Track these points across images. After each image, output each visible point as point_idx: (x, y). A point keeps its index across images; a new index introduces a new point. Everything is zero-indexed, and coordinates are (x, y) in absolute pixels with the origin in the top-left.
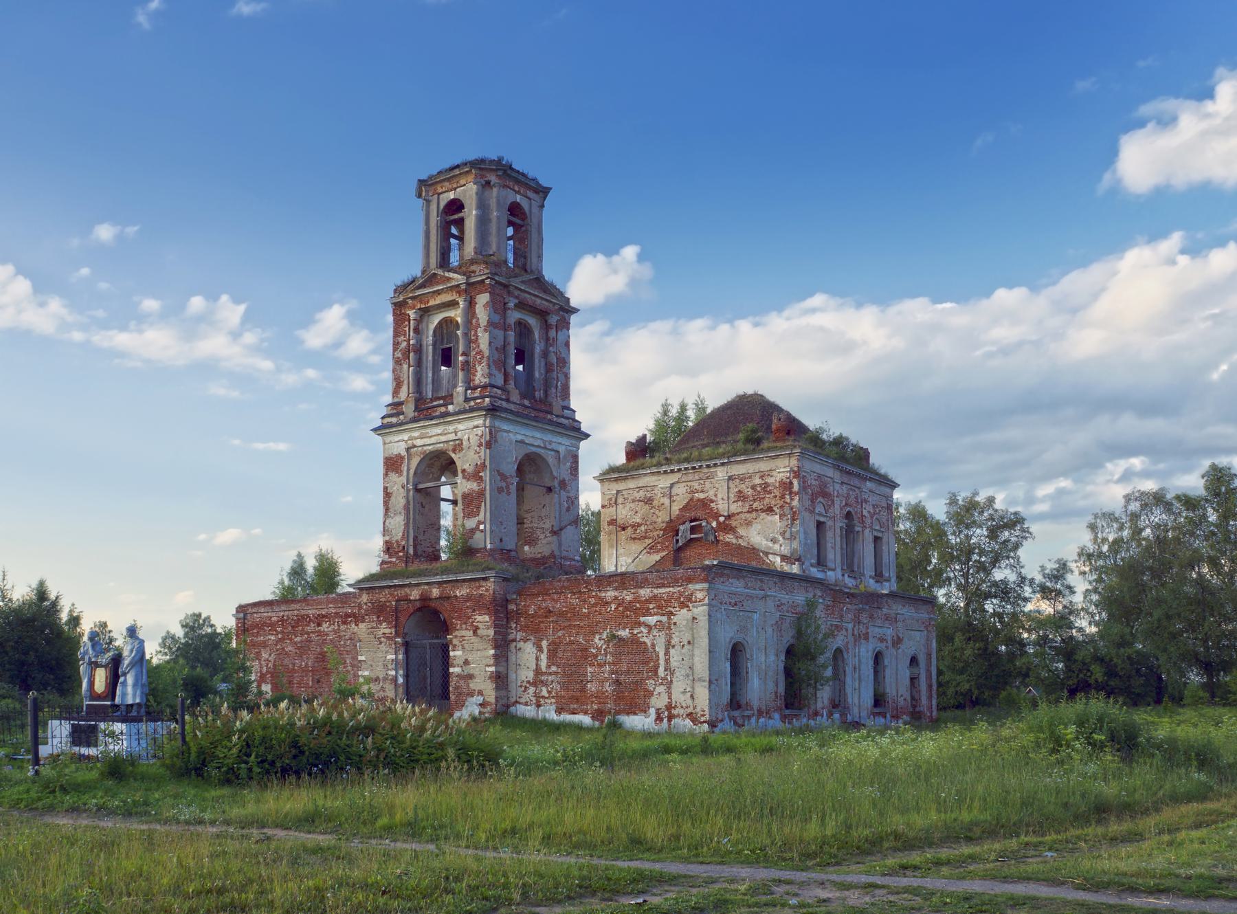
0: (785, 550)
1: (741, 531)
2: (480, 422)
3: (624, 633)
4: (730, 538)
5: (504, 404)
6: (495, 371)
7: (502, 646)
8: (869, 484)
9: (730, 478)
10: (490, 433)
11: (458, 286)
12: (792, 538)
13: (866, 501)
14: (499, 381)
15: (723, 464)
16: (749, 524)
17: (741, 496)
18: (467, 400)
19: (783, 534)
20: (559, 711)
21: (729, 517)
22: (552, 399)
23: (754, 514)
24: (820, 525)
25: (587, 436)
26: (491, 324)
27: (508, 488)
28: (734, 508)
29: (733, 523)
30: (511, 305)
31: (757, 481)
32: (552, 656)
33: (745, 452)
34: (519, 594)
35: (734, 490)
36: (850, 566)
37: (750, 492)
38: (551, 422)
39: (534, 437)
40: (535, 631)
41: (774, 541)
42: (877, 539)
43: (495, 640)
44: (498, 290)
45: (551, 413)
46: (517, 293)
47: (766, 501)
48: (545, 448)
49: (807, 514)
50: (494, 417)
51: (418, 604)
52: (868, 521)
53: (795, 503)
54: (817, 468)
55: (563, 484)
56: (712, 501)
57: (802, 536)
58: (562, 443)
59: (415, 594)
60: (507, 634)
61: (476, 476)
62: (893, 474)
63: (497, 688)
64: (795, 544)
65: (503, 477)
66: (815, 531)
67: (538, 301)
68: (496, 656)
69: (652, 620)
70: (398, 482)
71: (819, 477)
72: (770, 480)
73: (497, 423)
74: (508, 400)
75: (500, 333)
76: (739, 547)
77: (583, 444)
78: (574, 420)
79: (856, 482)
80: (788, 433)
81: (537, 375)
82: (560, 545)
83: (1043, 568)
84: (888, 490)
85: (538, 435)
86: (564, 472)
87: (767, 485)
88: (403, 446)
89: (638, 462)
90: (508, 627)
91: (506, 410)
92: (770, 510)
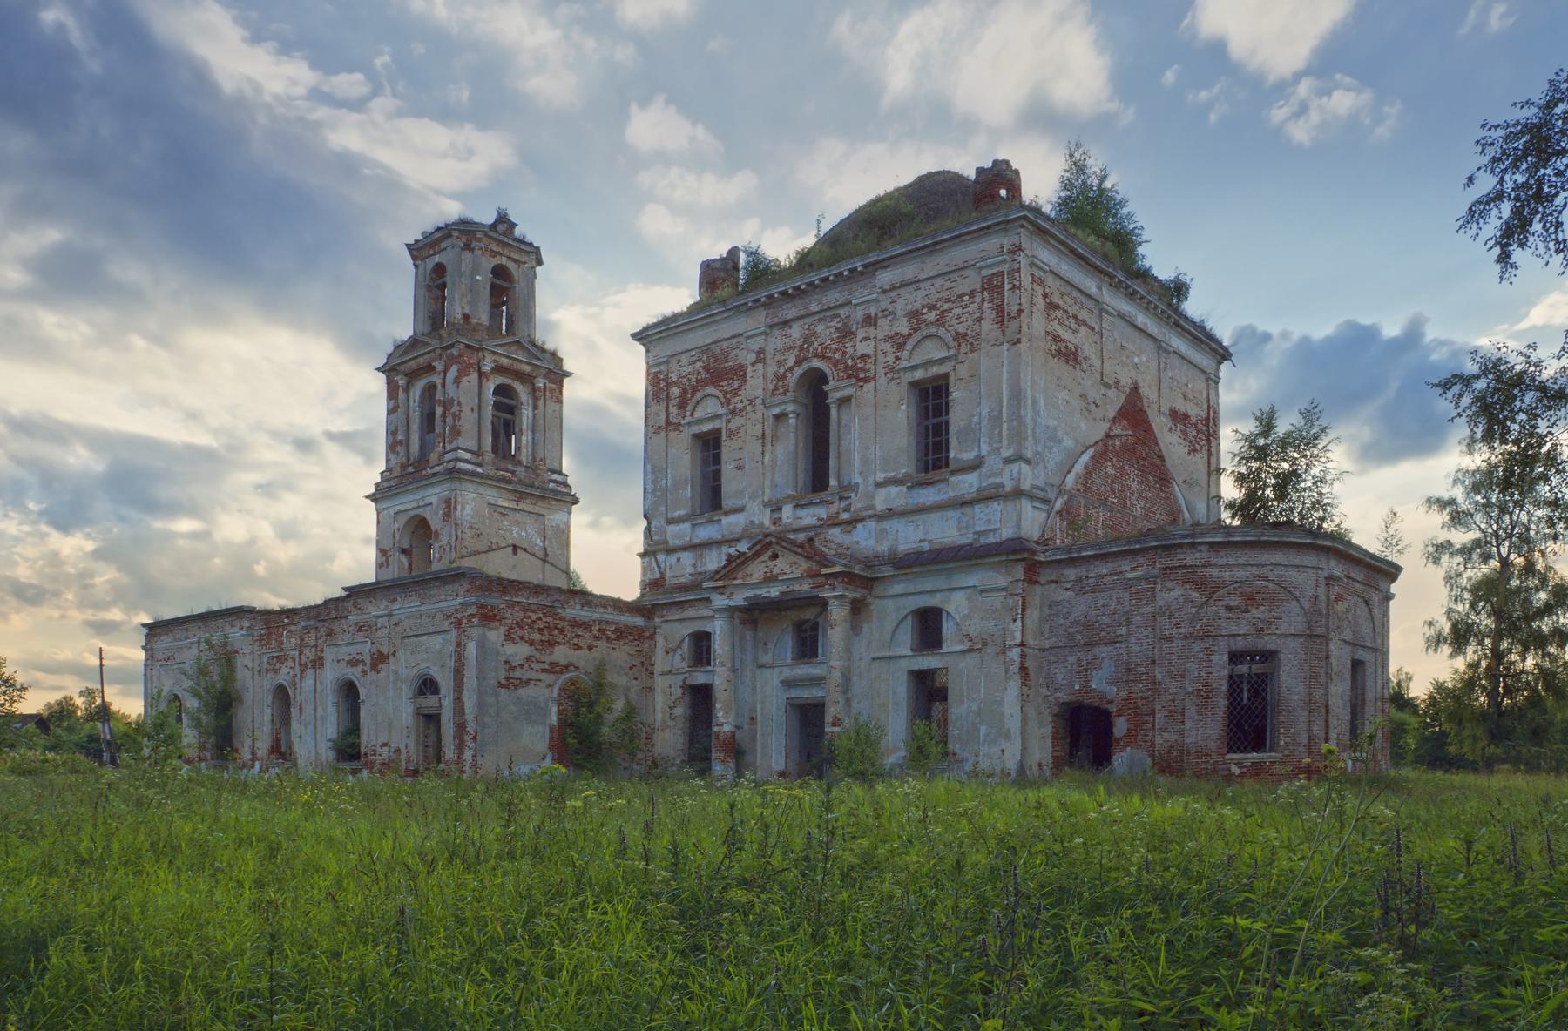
38: (428, 477)
85: (411, 497)
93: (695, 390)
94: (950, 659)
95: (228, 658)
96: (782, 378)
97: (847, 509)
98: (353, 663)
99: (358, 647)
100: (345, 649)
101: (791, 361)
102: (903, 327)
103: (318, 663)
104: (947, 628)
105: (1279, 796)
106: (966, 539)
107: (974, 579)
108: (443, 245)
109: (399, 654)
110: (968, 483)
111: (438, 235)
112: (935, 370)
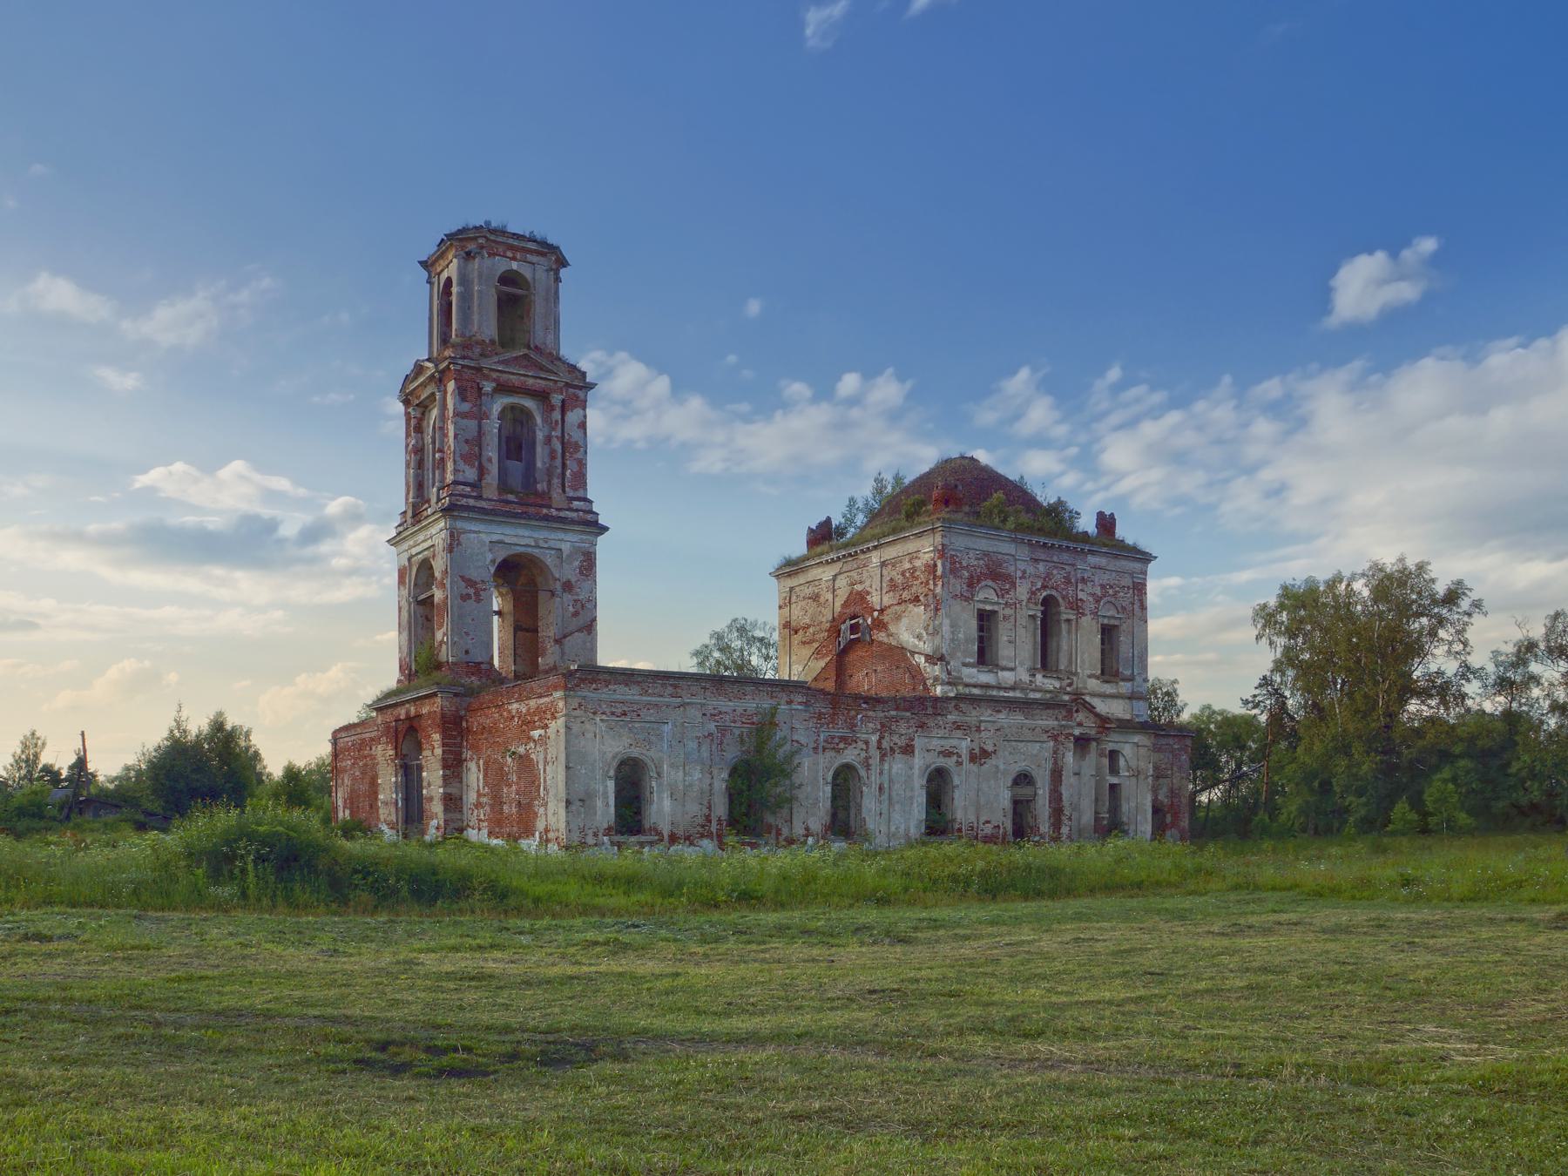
0: (927, 648)
1: (892, 628)
2: (442, 524)
3: (521, 750)
4: (881, 636)
5: (472, 502)
6: (462, 465)
7: (453, 766)
8: (1091, 559)
9: (883, 564)
10: (452, 535)
11: (432, 376)
12: (936, 632)
13: (1083, 580)
14: (470, 474)
15: (875, 547)
16: (898, 618)
17: (893, 586)
18: (439, 500)
19: (926, 629)
20: (490, 834)
21: (882, 611)
22: (556, 495)
23: (903, 607)
24: (986, 620)
25: (605, 529)
26: (456, 414)
27: (477, 594)
28: (887, 600)
29: (886, 618)
30: (488, 387)
31: (907, 566)
32: (485, 775)
33: (894, 531)
34: (467, 709)
35: (886, 579)
36: (1046, 660)
37: (899, 579)
38: (547, 518)
39: (519, 537)
40: (476, 748)
41: (919, 637)
42: (1108, 633)
43: (443, 759)
44: (468, 374)
45: (550, 507)
46: (495, 375)
47: (914, 590)
48: (537, 547)
49: (957, 606)
50: (455, 518)
51: (407, 724)
52: (1090, 605)
53: (938, 590)
54: (984, 545)
55: (568, 587)
56: (868, 593)
57: (946, 629)
58: (567, 541)
59: (402, 713)
60: (460, 753)
61: (443, 585)
62: (1145, 544)
63: (446, 810)
64: (937, 640)
65: (470, 583)
66: (974, 623)
67: (531, 381)
68: (445, 777)
69: (536, 734)
70: (405, 592)
71: (986, 554)
72: (918, 563)
73: (460, 524)
74: (479, 497)
75: (473, 424)
76: (891, 648)
77: (602, 541)
78: (591, 512)
79: (1065, 557)
80: (947, 503)
81: (539, 464)
82: (563, 653)
83: (1496, 653)
84: (1137, 566)
85: (527, 533)
86: (569, 572)
87: (914, 569)
88: (406, 555)
89: (819, 549)
90: (461, 746)
91: (468, 508)
92: (916, 600)
93: (979, 581)
94: (1123, 778)
95: (764, 727)
96: (1033, 593)
97: (1070, 685)
98: (947, 754)
99: (954, 742)
100: (935, 742)
101: (1039, 585)
102: (1098, 591)
103: (908, 750)
104: (1122, 762)
105: (983, 859)
106: (1128, 717)
107: (1136, 739)
108: (529, 257)
109: (1000, 753)
110: (1125, 688)
111: (531, 246)
112: (1113, 622)
